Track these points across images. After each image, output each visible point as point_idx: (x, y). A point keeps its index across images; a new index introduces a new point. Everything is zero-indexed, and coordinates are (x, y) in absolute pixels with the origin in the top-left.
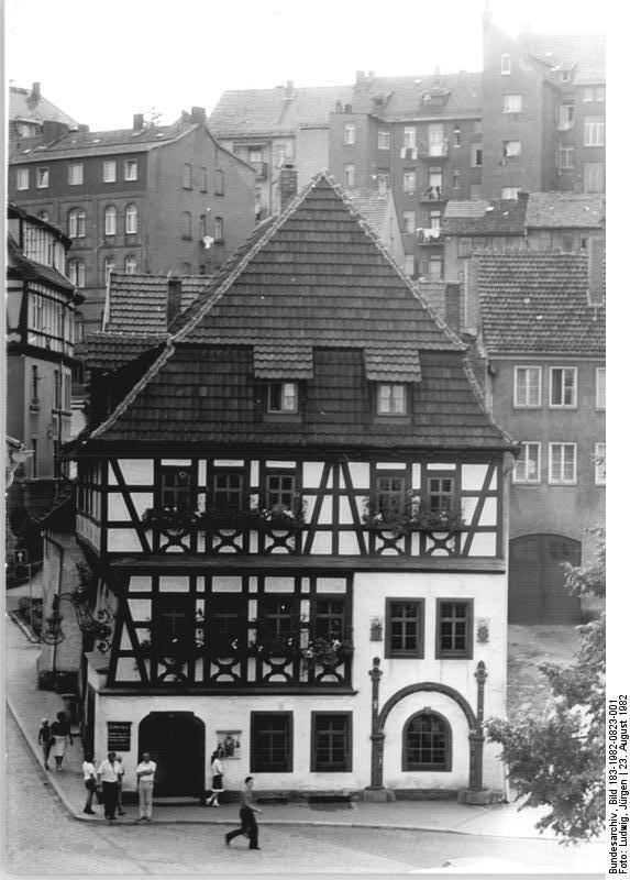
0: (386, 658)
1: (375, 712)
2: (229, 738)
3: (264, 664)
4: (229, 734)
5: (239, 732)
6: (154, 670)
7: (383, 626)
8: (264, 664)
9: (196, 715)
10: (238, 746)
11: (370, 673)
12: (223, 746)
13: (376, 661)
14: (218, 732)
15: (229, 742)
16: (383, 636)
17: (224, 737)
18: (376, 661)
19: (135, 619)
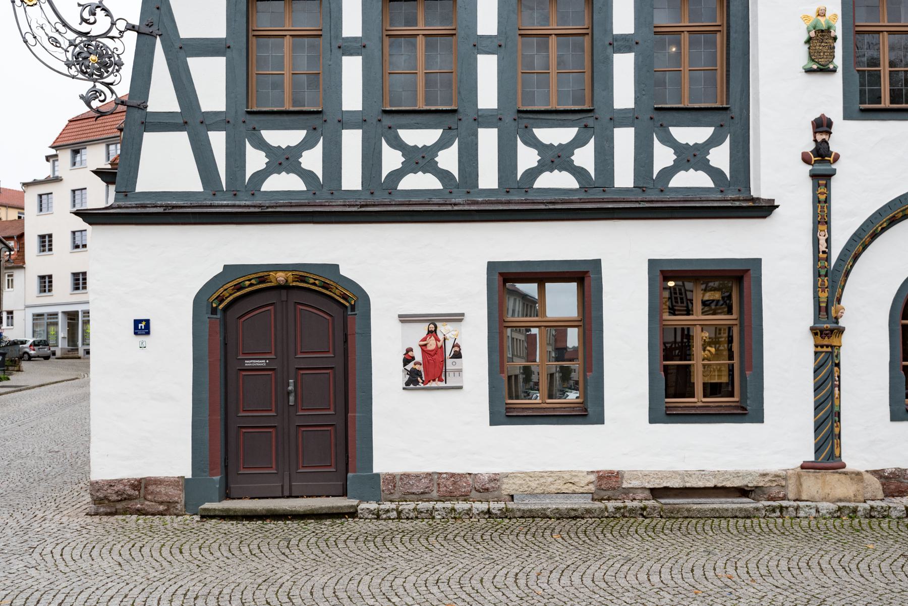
0: (848, 115)
1: (820, 256)
2: (432, 333)
3: (521, 146)
4: (433, 322)
5: (457, 318)
6: (236, 158)
7: (838, 31)
8: (521, 146)
9: (343, 272)
10: (458, 355)
11: (806, 159)
12: (418, 355)
13: (822, 125)
14: (405, 319)
15: (432, 344)
16: (838, 61)
17: (421, 330)
18: (822, 125)
19: (185, 32)
